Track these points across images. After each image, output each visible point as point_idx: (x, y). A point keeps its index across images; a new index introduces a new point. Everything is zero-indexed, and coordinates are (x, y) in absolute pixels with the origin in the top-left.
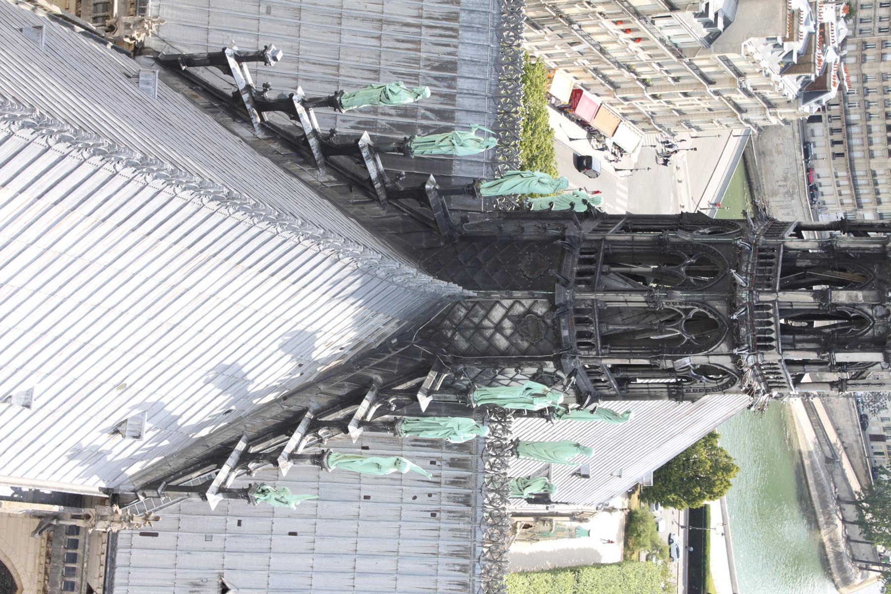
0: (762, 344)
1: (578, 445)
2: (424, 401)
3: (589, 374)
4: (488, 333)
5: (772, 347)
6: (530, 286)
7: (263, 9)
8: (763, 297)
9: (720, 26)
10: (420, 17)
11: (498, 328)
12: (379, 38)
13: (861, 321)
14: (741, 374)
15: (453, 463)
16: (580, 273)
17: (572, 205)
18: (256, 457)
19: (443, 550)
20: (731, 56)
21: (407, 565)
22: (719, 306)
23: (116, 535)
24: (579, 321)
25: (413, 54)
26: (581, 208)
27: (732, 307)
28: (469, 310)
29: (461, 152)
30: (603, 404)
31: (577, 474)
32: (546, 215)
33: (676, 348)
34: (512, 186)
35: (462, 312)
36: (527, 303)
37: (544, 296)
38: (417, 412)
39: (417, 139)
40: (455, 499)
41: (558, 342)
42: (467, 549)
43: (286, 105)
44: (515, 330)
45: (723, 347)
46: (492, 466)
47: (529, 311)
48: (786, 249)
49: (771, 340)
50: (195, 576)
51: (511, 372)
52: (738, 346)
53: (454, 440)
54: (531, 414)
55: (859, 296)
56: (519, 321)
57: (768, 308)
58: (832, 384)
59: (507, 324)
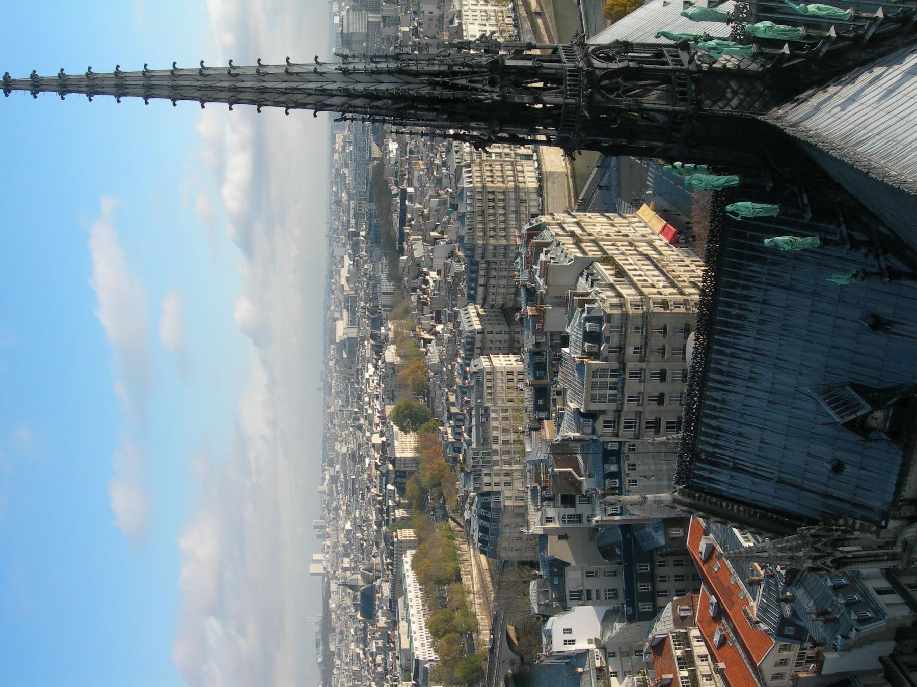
0: (576, 72)
2: (786, 50)
3: (680, 61)
4: (742, 90)
5: (569, 71)
6: (714, 117)
7: (862, 303)
8: (573, 101)
9: (585, 274)
10: (766, 290)
11: (735, 93)
12: (792, 279)
13: (516, 84)
14: (587, 55)
16: (681, 124)
17: (683, 166)
20: (580, 255)
22: (599, 98)
25: (773, 267)
26: (678, 164)
27: (590, 98)
28: (752, 106)
29: (749, 204)
30: (672, 42)
32: (698, 162)
33: (625, 73)
34: (720, 180)
35: (757, 105)
37: (706, 111)
38: (792, 44)
39: (775, 214)
43: (855, 245)
44: (724, 92)
45: (598, 72)
46: (745, 7)
47: (715, 102)
48: (557, 129)
49: (569, 76)
51: (729, 65)
53: (768, 24)
54: (719, 38)
55: (516, 100)
56: (723, 97)
57: (570, 95)
58: (535, 48)
59: (729, 95)
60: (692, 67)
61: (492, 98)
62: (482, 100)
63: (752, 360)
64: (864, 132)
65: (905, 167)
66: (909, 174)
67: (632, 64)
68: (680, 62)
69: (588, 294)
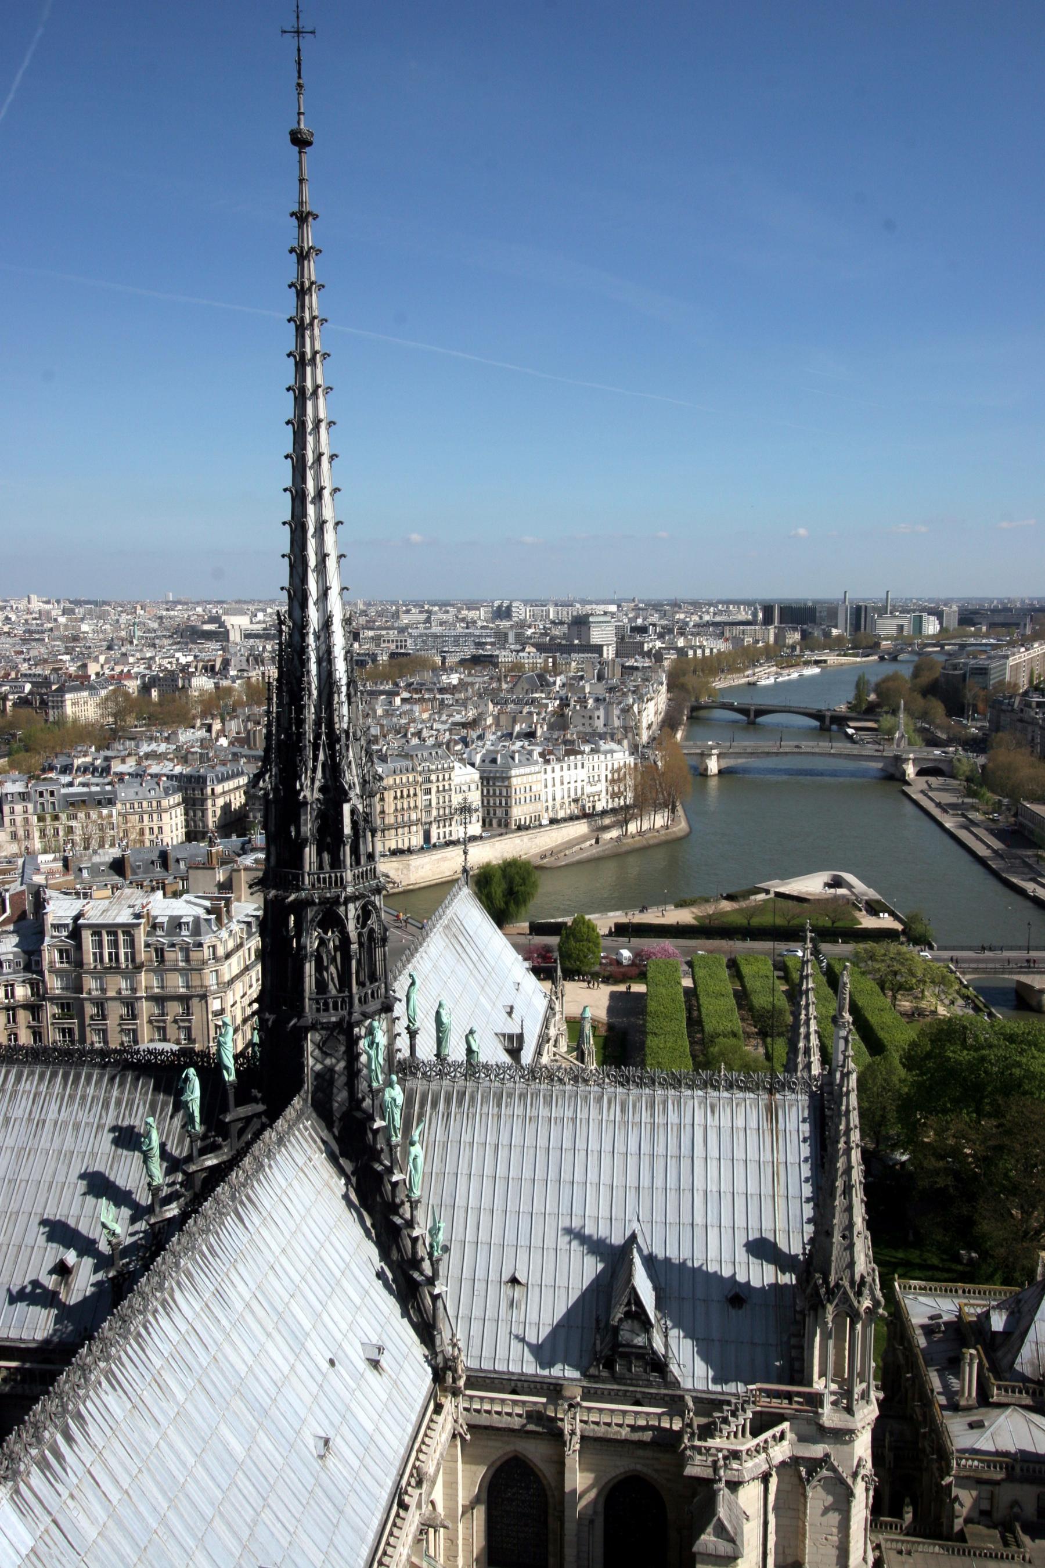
1: (438, 1013)
2: (378, 1124)
15: (435, 1104)
18: (414, 1252)
19: (496, 1110)
21: (504, 1139)
23: (468, 1369)
24: (326, 1010)
29: (197, 1093)
31: (510, 1014)
33: (345, 941)
36: (310, 1047)
40: (460, 1103)
41: (338, 1024)
42: (495, 1094)
44: (330, 1055)
45: (342, 908)
50: (504, 1305)
51: (364, 1058)
52: (339, 897)
53: (400, 1099)
58: (373, 836)
60: (356, 1016)
61: (302, 789)
62: (300, 778)
63: (29, 1120)
64: (257, 1222)
65: (189, 1275)
66: (179, 1284)
67: (354, 947)
68: (363, 1001)
69: (230, 918)
